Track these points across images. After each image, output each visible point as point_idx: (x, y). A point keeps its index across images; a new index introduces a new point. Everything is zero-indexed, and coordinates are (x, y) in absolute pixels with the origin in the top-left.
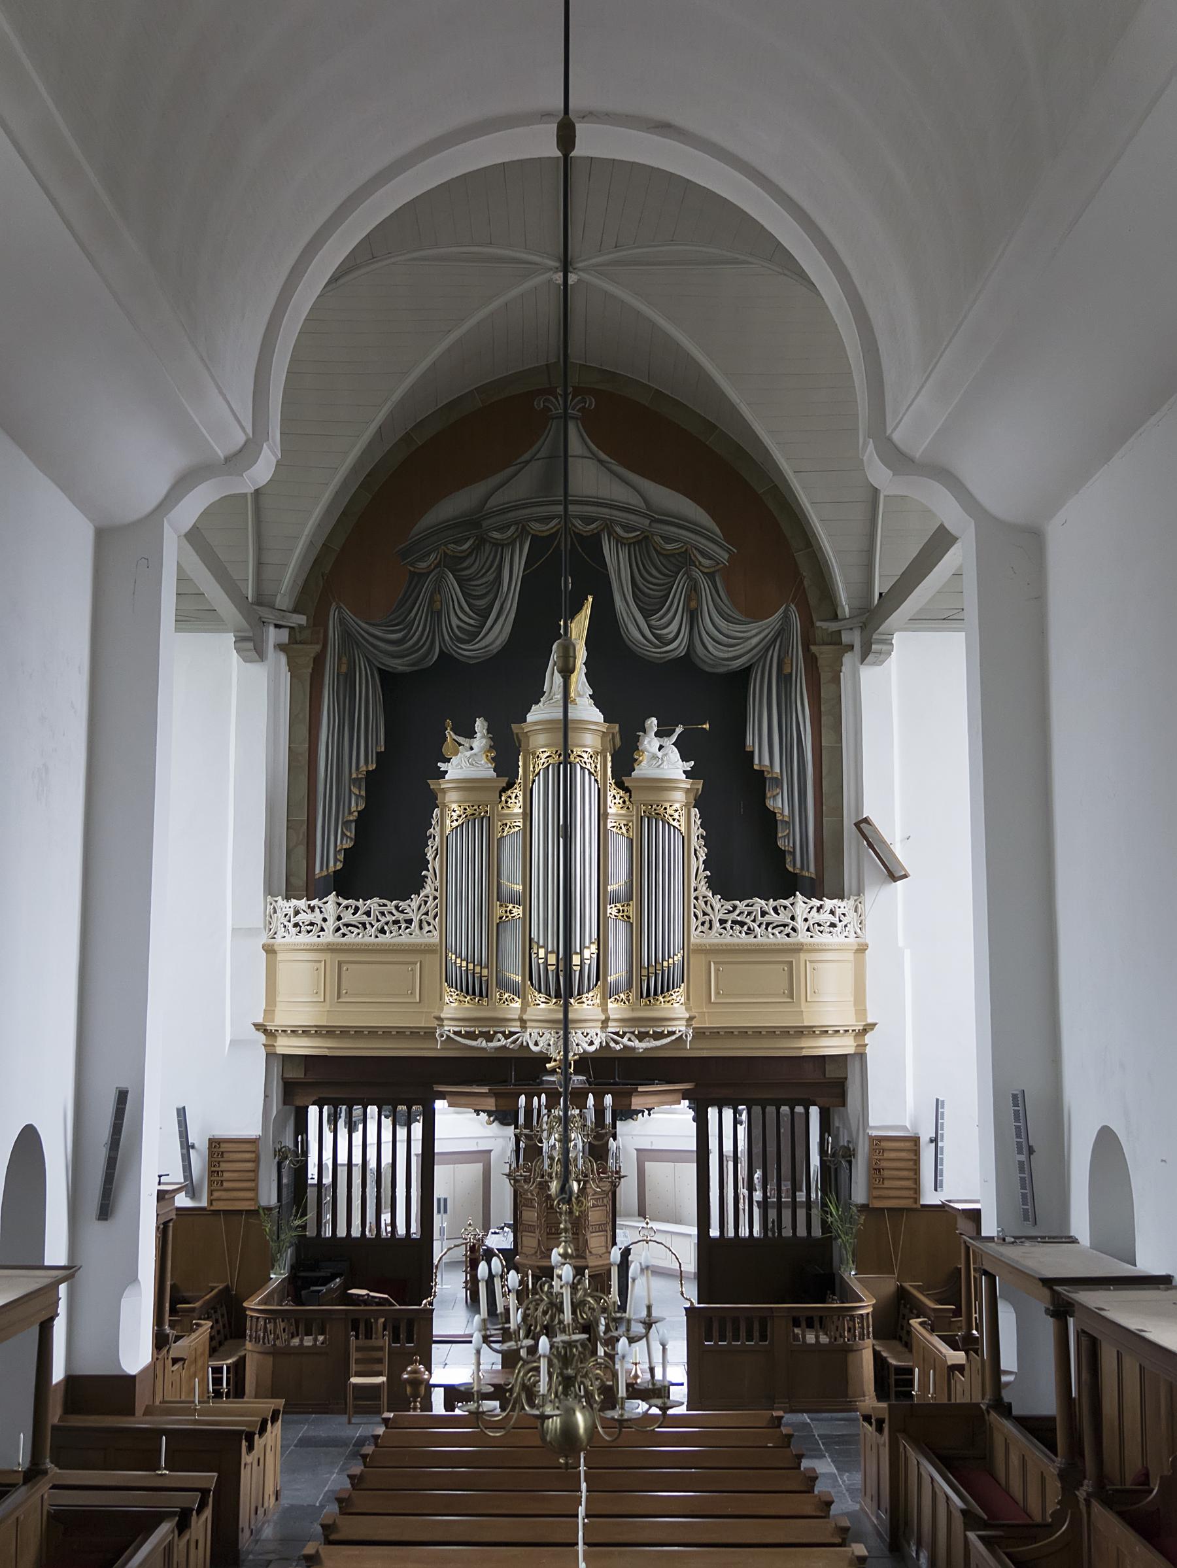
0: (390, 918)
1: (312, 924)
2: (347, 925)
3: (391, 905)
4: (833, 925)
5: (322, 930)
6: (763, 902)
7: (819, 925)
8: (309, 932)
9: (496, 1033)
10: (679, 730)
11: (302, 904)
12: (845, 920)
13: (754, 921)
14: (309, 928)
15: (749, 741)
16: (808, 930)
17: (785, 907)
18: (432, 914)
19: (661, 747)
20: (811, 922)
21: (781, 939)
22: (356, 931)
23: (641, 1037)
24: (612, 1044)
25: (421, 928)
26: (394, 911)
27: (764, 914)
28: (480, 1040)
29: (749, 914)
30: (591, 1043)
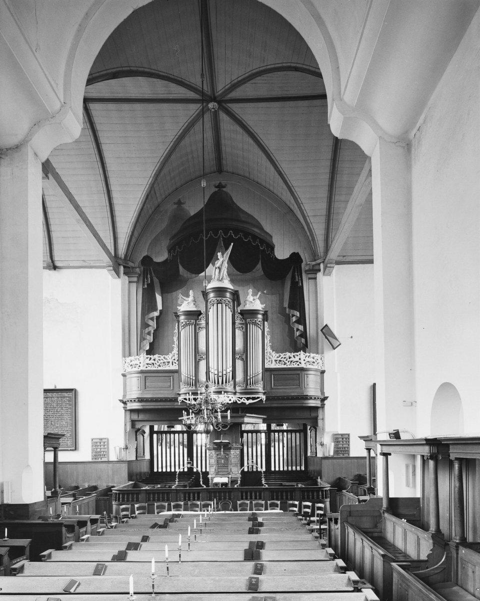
0: (162, 361)
3: (162, 357)
4: (314, 362)
5: (140, 366)
7: (309, 362)
10: (259, 293)
12: (318, 362)
13: (287, 360)
16: (305, 364)
17: (297, 355)
18: (176, 360)
19: (254, 300)
20: (306, 361)
21: (296, 366)
22: (150, 365)
23: (248, 399)
25: (173, 365)
27: (290, 358)
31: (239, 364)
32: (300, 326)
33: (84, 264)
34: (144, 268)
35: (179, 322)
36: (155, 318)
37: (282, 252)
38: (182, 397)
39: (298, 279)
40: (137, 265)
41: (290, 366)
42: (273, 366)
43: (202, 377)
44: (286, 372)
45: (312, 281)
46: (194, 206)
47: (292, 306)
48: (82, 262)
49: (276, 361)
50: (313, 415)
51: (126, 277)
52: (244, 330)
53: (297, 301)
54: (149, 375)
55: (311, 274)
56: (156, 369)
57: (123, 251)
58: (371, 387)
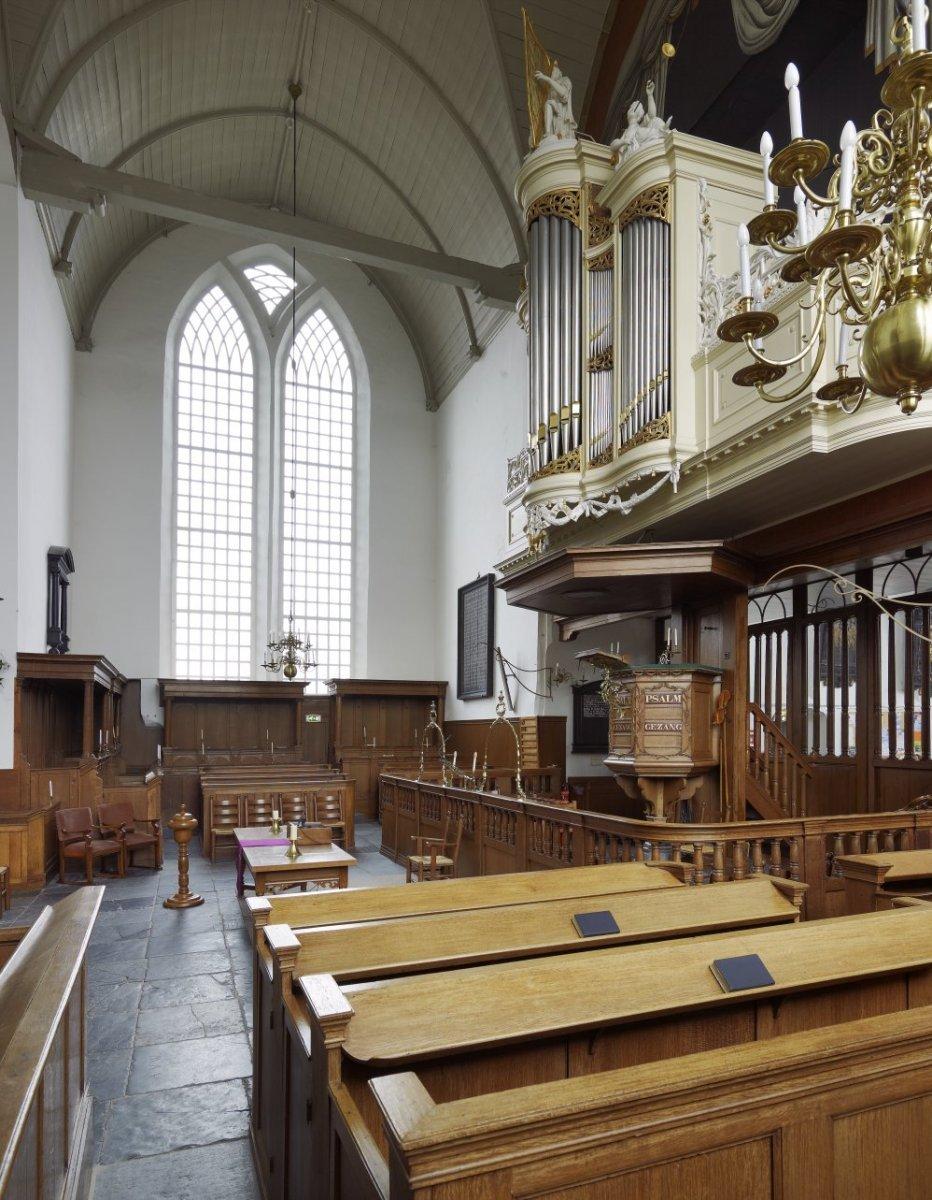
15: (869, 42)
23: (625, 494)
24: (594, 511)
30: (561, 515)
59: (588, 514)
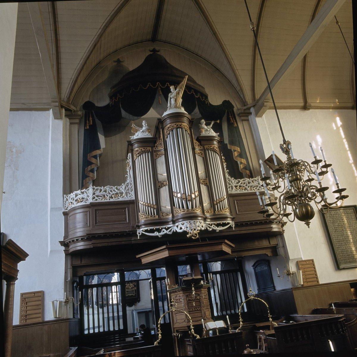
0: (114, 192)
1: (83, 198)
2: (97, 196)
3: (114, 188)
5: (87, 200)
6: (248, 179)
8: (82, 202)
9: (162, 228)
10: (212, 123)
11: (79, 192)
13: (246, 185)
14: (82, 200)
17: (256, 180)
22: (101, 198)
23: (218, 225)
26: (116, 190)
27: (249, 183)
28: (156, 232)
29: (244, 183)
31: (204, 188)
32: (242, 159)
33: (24, 106)
34: (86, 112)
35: (132, 151)
36: (98, 156)
37: (215, 99)
38: (141, 229)
39: (233, 121)
40: (78, 108)
41: (251, 191)
42: (234, 192)
43: (166, 206)
44: (247, 197)
45: (245, 123)
46: (133, 63)
47: (232, 143)
48: (20, 104)
49: (236, 186)
50: (273, 242)
51: (68, 120)
52: (203, 156)
53: (236, 139)
54: (100, 208)
55: (244, 116)
56: (108, 200)
57: (66, 94)
58: (318, 212)
59: (206, 228)
